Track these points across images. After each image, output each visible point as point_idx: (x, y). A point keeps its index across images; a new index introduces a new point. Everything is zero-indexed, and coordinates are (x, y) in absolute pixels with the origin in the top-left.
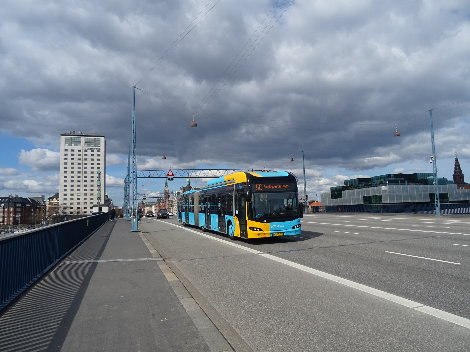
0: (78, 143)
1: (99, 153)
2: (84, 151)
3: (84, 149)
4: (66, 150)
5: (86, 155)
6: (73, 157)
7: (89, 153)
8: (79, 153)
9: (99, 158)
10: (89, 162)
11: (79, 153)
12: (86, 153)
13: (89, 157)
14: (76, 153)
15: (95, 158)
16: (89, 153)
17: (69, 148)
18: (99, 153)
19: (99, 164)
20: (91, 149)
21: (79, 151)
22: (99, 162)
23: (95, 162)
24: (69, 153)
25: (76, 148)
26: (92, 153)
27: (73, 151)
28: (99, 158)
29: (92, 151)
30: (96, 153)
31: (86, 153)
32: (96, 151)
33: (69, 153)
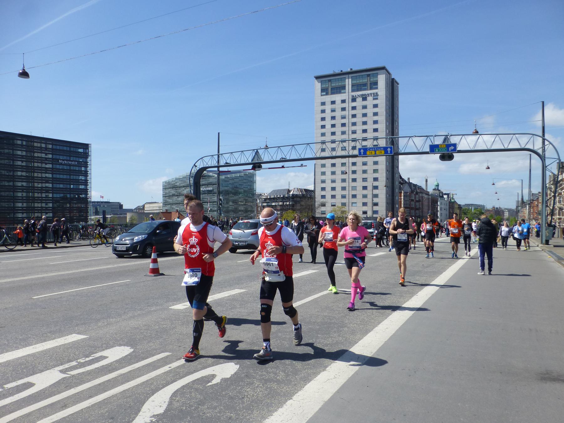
0: (340, 89)
1: (375, 102)
2: (350, 100)
3: (351, 97)
4: (323, 104)
5: (354, 108)
6: (333, 114)
7: (359, 103)
8: (344, 105)
9: (376, 110)
10: (359, 119)
11: (344, 105)
12: (354, 104)
13: (359, 112)
14: (339, 105)
15: (370, 111)
16: (359, 103)
17: (328, 98)
18: (375, 102)
19: (375, 122)
20: (362, 95)
21: (343, 101)
22: (376, 118)
23: (370, 119)
24: (328, 107)
25: (338, 98)
26: (365, 103)
27: (333, 103)
28: (376, 110)
29: (364, 98)
30: (370, 101)
31: (354, 104)
32: (370, 99)
33: (328, 107)
